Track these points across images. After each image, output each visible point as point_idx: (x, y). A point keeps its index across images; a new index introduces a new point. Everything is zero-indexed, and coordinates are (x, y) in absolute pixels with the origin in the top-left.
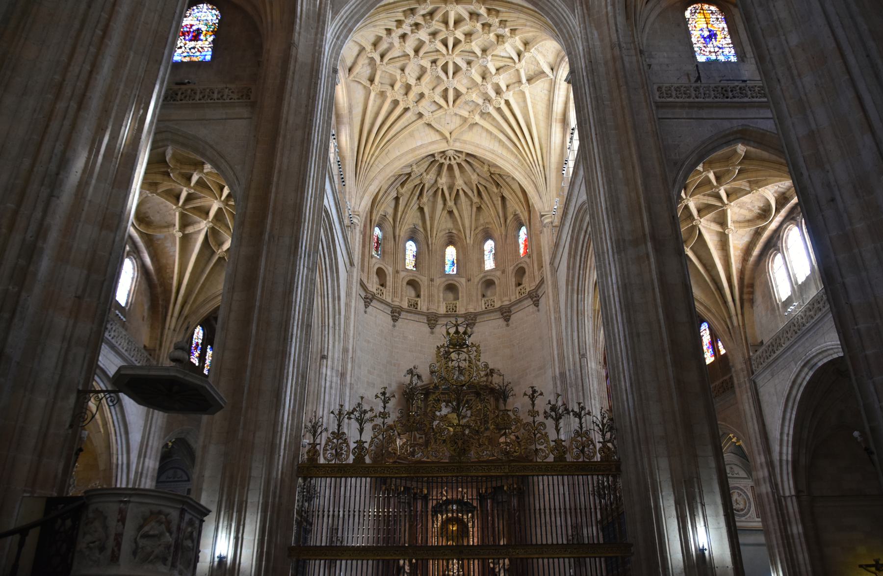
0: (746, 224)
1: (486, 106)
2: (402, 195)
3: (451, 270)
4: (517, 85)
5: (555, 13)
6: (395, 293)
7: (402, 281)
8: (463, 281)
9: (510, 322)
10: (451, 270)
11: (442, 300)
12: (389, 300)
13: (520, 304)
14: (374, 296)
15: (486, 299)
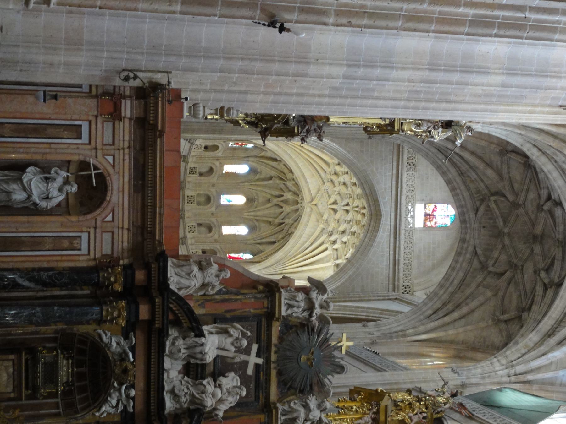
1: (326, 233)
2: (279, 164)
3: (225, 200)
4: (335, 256)
5: (331, 282)
6: (200, 157)
7: (211, 163)
8: (213, 209)
10: (225, 200)
11: (198, 192)
12: (192, 154)
14: (192, 144)
15: (196, 226)
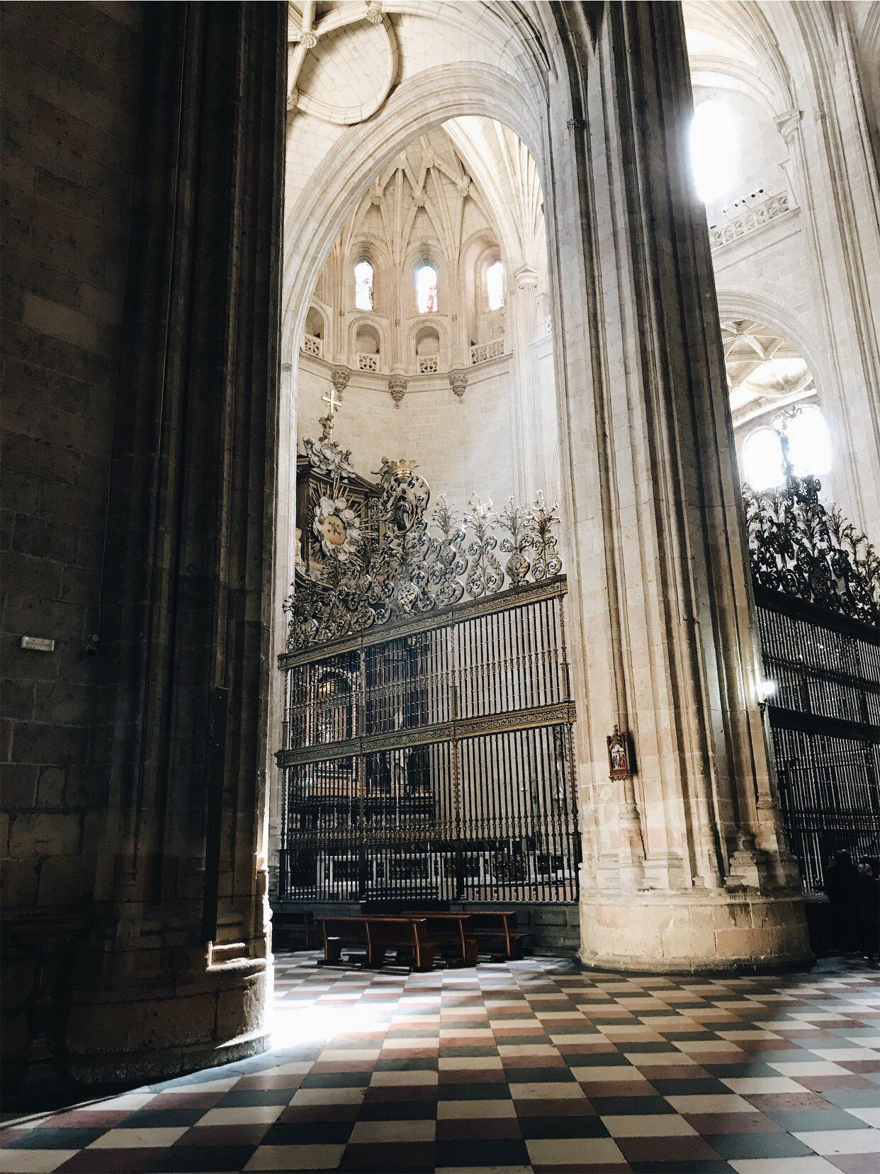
0: (756, 388)
5: (806, 15)
9: (402, 403)
13: (426, 382)
